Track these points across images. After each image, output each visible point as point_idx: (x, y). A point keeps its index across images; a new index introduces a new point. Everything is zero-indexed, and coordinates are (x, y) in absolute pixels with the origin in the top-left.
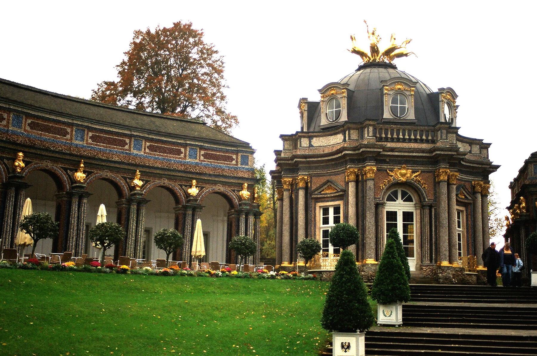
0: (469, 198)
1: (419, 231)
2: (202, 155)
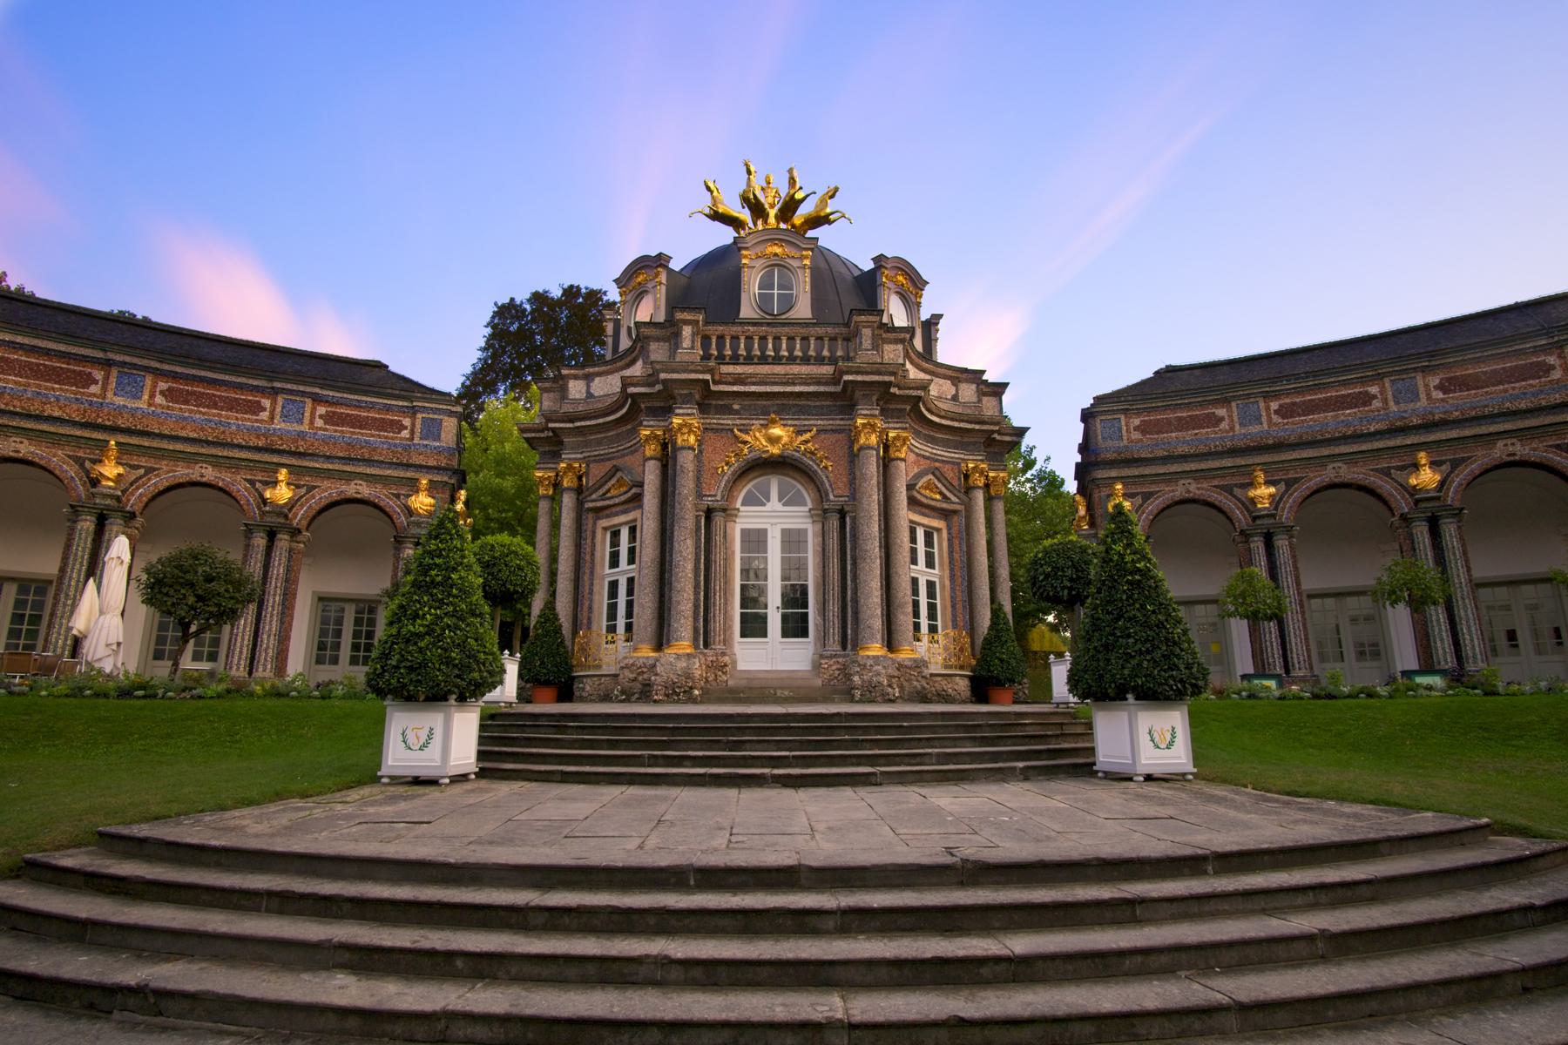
0: (954, 499)
1: (819, 574)
2: (321, 417)
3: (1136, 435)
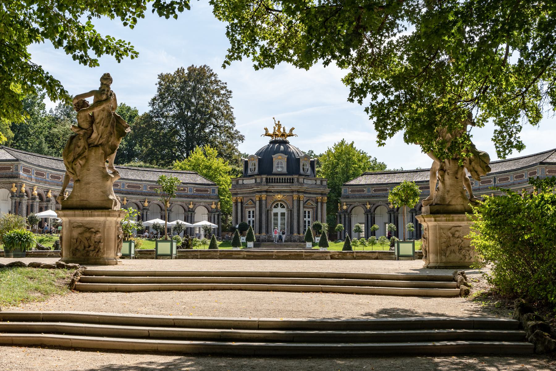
3: (350, 193)
